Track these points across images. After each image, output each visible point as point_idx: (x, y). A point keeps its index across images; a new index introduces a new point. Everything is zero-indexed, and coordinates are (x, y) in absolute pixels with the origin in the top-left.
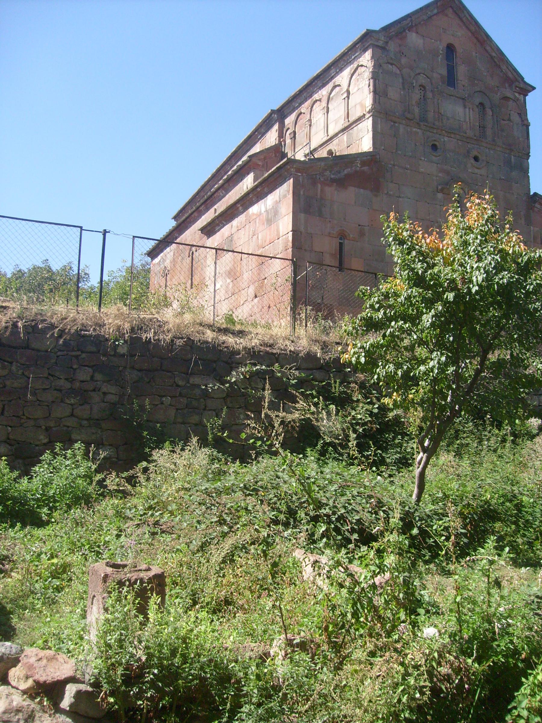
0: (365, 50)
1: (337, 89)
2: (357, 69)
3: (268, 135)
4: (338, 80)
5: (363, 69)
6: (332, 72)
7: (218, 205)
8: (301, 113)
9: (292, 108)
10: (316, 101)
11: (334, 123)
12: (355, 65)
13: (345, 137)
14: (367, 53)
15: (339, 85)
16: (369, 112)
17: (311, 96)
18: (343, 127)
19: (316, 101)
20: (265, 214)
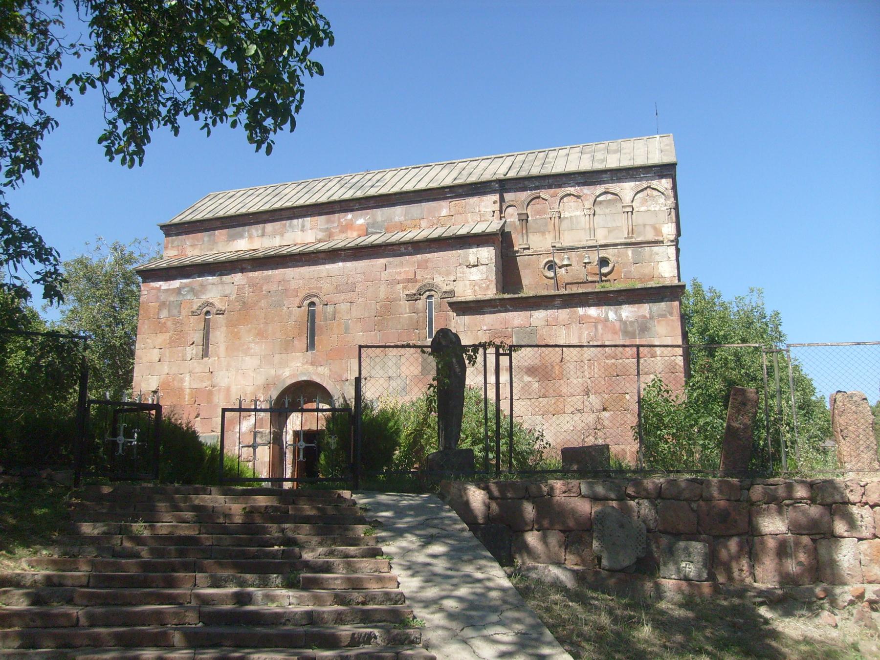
0: (661, 177)
1: (610, 197)
2: (646, 189)
3: (473, 201)
4: (614, 187)
5: (655, 193)
6: (605, 177)
7: (391, 259)
8: (539, 197)
9: (520, 186)
10: (569, 195)
11: (606, 230)
12: (645, 184)
13: (629, 252)
14: (664, 181)
15: (617, 195)
16: (672, 241)
17: (560, 186)
18: (628, 241)
19: (569, 195)
20: (617, 324)
